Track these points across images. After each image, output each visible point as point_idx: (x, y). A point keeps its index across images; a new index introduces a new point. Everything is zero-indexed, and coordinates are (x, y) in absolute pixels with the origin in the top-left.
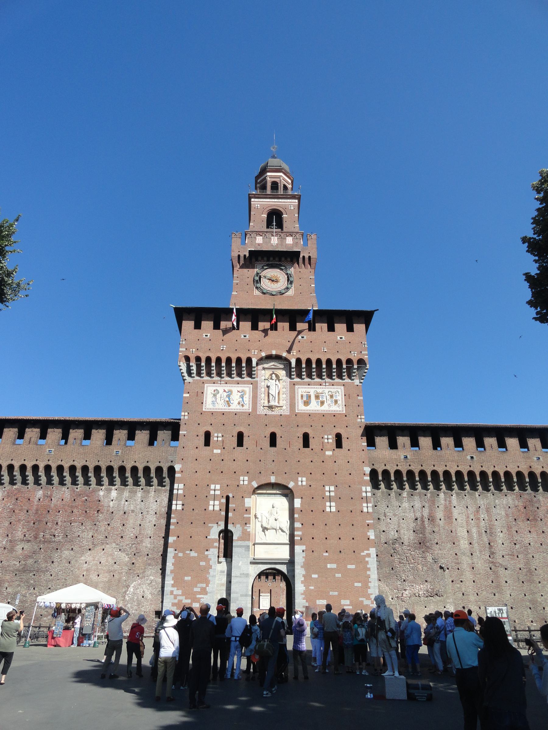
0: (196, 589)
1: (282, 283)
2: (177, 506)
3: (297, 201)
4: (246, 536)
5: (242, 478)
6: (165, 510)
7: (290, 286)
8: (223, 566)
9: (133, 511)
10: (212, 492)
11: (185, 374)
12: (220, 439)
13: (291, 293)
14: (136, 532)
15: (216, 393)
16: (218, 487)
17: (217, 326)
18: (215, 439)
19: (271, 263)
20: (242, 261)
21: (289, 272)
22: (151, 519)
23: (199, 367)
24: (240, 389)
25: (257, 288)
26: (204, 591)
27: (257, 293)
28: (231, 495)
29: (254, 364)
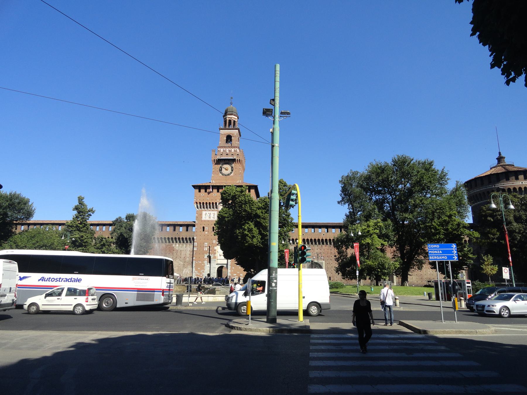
0: (201, 271)
1: (230, 170)
2: (195, 249)
3: (238, 131)
4: (215, 257)
5: (214, 241)
6: (192, 250)
7: (232, 172)
8: (209, 265)
9: (183, 250)
10: (205, 245)
11: (196, 208)
12: (207, 229)
13: (232, 174)
14: (184, 256)
15: (206, 214)
16: (207, 243)
17: (206, 191)
18: (206, 229)
19: (226, 162)
20: (216, 162)
21: (232, 166)
22: (188, 252)
23: (200, 206)
24: (213, 213)
25: (220, 173)
26: (203, 272)
27: (221, 175)
28: (210, 246)
29: (218, 204)
